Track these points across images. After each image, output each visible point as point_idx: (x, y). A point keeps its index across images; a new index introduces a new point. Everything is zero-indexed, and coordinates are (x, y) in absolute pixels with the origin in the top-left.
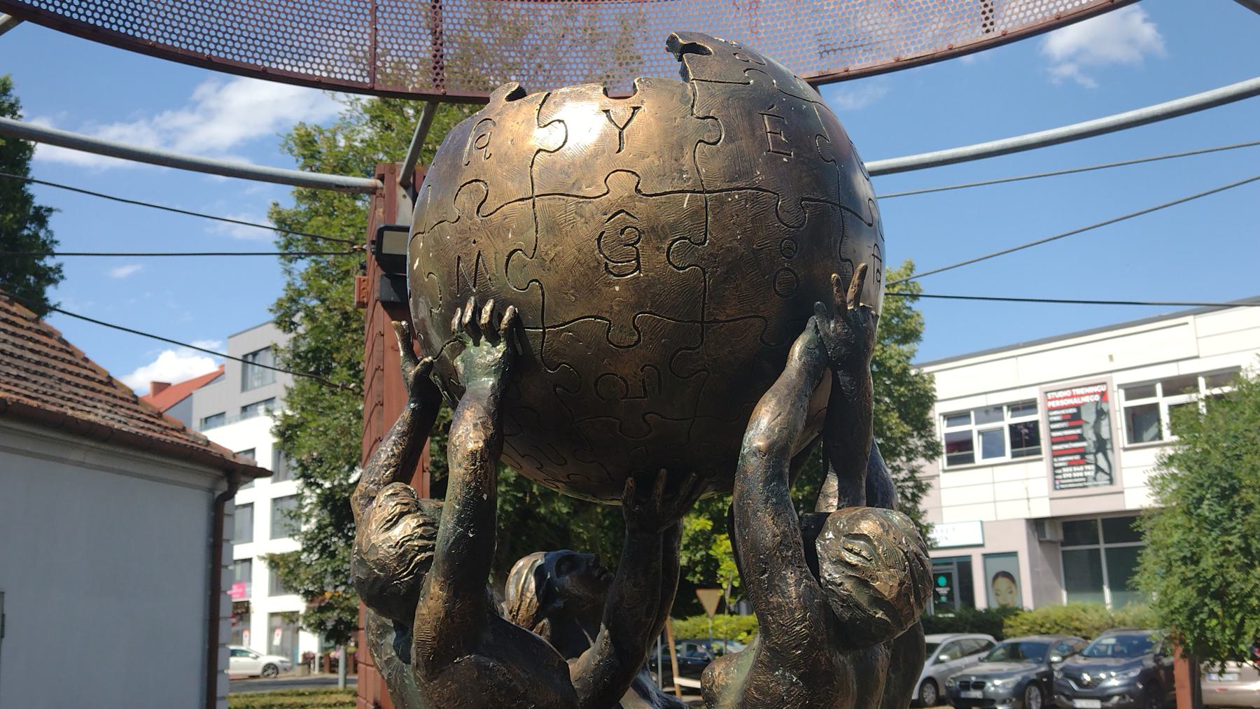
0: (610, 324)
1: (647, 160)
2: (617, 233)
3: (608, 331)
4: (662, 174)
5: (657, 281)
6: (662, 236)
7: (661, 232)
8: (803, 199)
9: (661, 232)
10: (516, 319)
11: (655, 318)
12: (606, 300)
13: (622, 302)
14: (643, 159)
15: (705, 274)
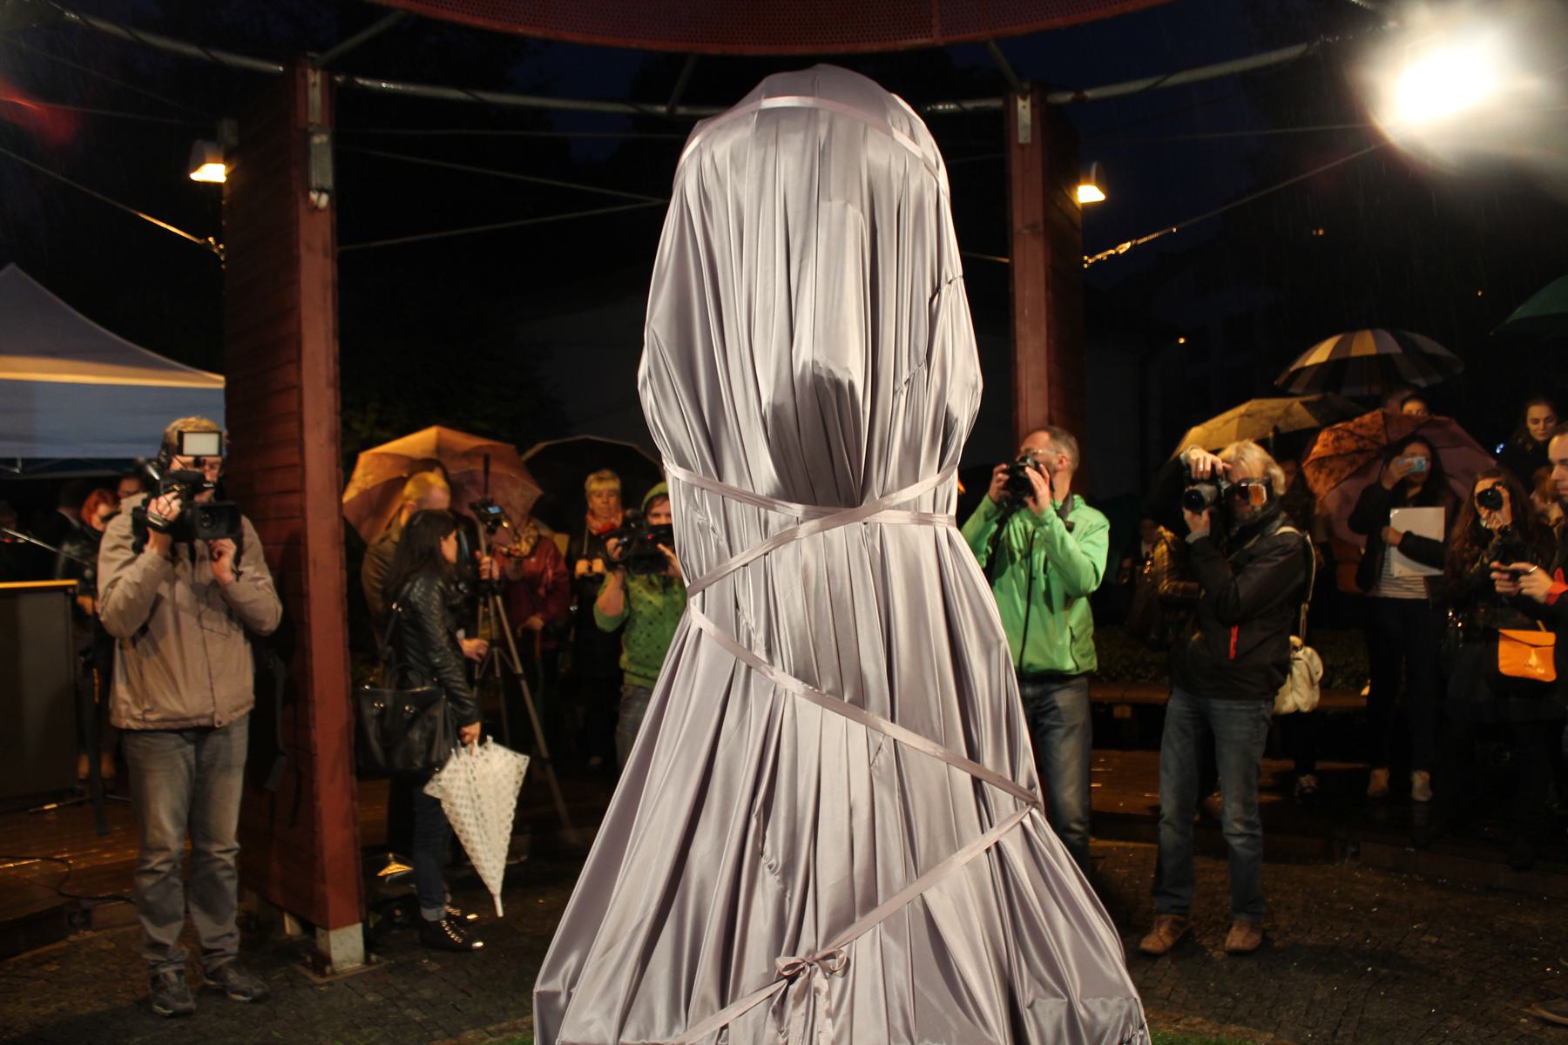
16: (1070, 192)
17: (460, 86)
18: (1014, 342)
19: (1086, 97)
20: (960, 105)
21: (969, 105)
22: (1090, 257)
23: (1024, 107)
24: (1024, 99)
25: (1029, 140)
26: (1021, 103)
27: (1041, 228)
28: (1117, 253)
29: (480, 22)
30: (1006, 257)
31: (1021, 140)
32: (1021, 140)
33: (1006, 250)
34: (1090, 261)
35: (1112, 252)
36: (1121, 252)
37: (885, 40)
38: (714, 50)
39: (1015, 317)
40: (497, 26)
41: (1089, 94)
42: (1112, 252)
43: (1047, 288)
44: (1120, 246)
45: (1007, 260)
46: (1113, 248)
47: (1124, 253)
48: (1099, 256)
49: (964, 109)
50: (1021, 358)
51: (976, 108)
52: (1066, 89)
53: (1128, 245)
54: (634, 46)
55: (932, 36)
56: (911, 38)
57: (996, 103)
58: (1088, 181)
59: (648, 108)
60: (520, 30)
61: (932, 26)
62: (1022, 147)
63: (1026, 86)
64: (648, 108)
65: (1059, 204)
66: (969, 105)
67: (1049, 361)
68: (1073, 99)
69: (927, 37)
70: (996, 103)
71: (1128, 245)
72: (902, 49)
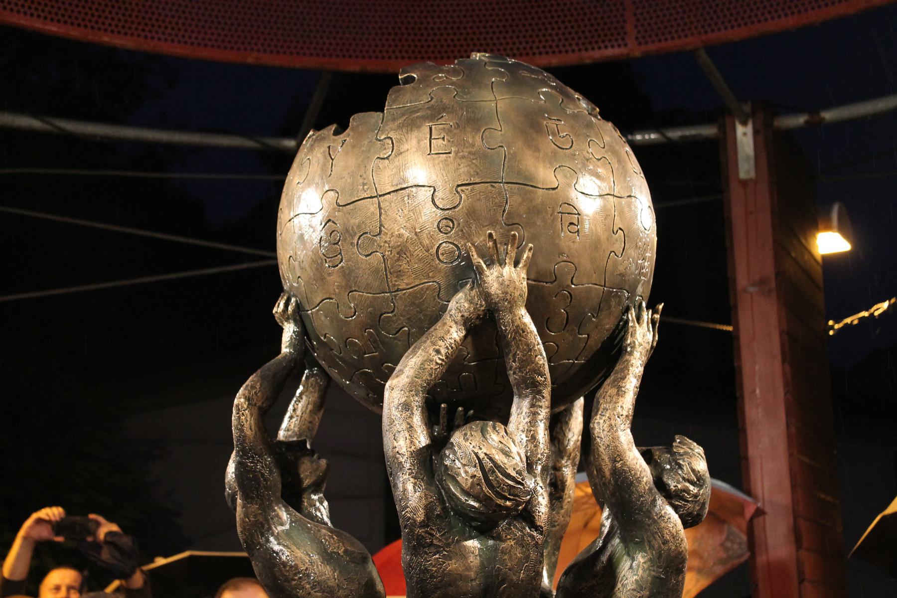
0: (338, 304)
1: (343, 180)
2: (328, 237)
3: (338, 308)
4: (351, 188)
5: (354, 268)
6: (353, 234)
7: (351, 231)
8: (458, 186)
9: (351, 231)
10: (298, 306)
11: (359, 295)
12: (331, 285)
13: (338, 286)
14: (342, 179)
15: (383, 256)
16: (806, 240)
17: (35, 115)
18: (744, 431)
19: (824, 119)
20: (663, 134)
21: (675, 134)
22: (837, 321)
23: (745, 134)
24: (744, 123)
25: (752, 174)
26: (740, 129)
27: (773, 285)
28: (872, 315)
29: (53, 28)
30: (729, 324)
31: (743, 175)
32: (743, 175)
33: (727, 314)
34: (837, 326)
35: (865, 314)
36: (876, 314)
37: (567, 51)
38: (353, 66)
39: (742, 397)
40: (75, 33)
41: (828, 115)
42: (865, 314)
43: (784, 361)
44: (875, 307)
45: (730, 328)
46: (867, 310)
47: (879, 315)
48: (848, 320)
49: (668, 139)
50: (752, 452)
51: (683, 138)
52: (796, 110)
53: (885, 305)
54: (250, 60)
55: (626, 45)
56: (600, 48)
57: (708, 131)
58: (828, 227)
59: (272, 142)
60: (106, 39)
61: (625, 33)
62: (744, 183)
63: (747, 108)
64: (272, 142)
65: (793, 254)
66: (675, 134)
67: (791, 455)
68: (806, 122)
69: (619, 46)
70: (708, 131)
71: (885, 305)
72: (588, 61)
